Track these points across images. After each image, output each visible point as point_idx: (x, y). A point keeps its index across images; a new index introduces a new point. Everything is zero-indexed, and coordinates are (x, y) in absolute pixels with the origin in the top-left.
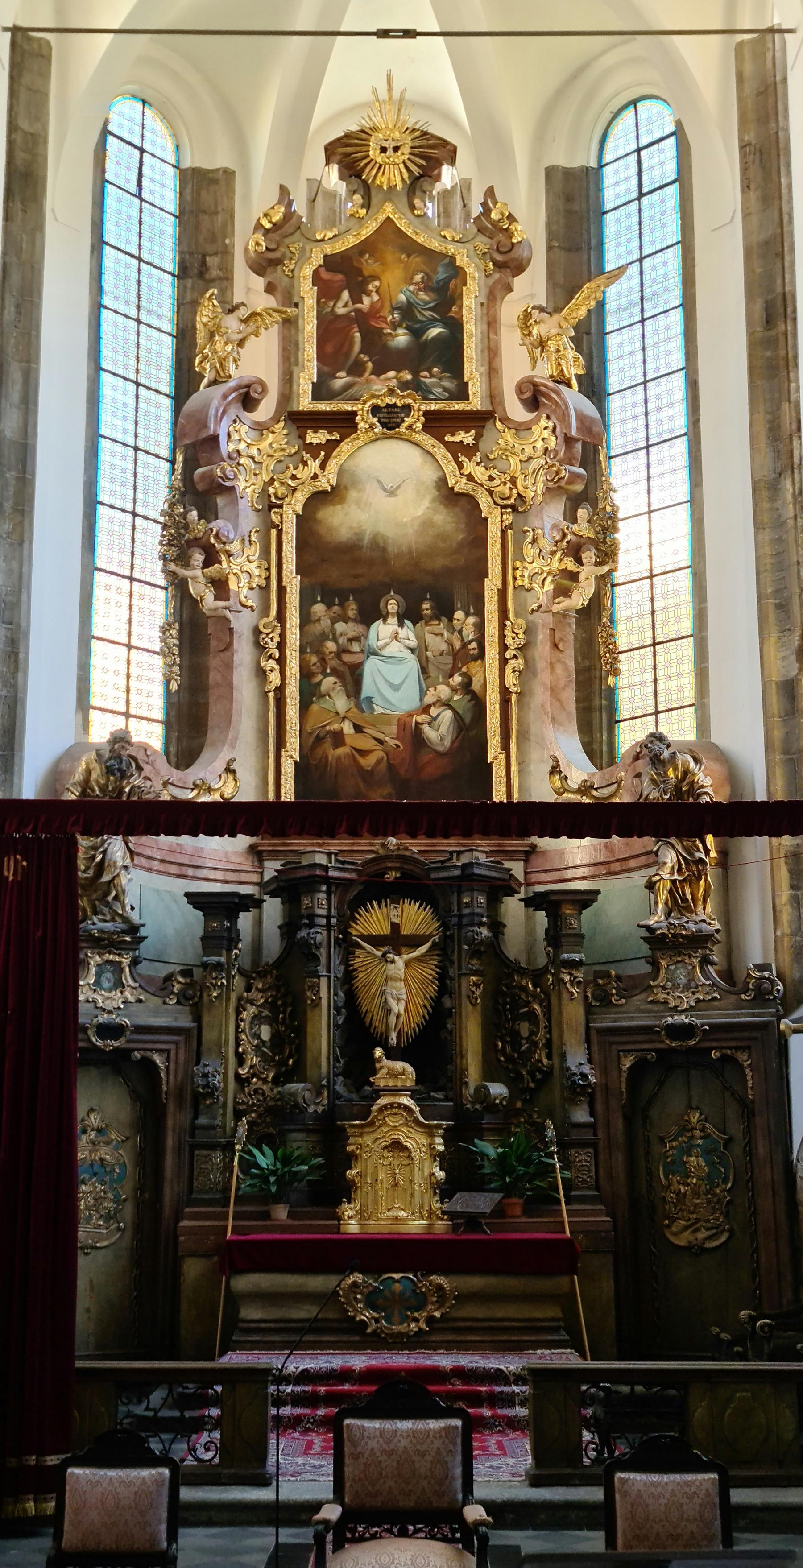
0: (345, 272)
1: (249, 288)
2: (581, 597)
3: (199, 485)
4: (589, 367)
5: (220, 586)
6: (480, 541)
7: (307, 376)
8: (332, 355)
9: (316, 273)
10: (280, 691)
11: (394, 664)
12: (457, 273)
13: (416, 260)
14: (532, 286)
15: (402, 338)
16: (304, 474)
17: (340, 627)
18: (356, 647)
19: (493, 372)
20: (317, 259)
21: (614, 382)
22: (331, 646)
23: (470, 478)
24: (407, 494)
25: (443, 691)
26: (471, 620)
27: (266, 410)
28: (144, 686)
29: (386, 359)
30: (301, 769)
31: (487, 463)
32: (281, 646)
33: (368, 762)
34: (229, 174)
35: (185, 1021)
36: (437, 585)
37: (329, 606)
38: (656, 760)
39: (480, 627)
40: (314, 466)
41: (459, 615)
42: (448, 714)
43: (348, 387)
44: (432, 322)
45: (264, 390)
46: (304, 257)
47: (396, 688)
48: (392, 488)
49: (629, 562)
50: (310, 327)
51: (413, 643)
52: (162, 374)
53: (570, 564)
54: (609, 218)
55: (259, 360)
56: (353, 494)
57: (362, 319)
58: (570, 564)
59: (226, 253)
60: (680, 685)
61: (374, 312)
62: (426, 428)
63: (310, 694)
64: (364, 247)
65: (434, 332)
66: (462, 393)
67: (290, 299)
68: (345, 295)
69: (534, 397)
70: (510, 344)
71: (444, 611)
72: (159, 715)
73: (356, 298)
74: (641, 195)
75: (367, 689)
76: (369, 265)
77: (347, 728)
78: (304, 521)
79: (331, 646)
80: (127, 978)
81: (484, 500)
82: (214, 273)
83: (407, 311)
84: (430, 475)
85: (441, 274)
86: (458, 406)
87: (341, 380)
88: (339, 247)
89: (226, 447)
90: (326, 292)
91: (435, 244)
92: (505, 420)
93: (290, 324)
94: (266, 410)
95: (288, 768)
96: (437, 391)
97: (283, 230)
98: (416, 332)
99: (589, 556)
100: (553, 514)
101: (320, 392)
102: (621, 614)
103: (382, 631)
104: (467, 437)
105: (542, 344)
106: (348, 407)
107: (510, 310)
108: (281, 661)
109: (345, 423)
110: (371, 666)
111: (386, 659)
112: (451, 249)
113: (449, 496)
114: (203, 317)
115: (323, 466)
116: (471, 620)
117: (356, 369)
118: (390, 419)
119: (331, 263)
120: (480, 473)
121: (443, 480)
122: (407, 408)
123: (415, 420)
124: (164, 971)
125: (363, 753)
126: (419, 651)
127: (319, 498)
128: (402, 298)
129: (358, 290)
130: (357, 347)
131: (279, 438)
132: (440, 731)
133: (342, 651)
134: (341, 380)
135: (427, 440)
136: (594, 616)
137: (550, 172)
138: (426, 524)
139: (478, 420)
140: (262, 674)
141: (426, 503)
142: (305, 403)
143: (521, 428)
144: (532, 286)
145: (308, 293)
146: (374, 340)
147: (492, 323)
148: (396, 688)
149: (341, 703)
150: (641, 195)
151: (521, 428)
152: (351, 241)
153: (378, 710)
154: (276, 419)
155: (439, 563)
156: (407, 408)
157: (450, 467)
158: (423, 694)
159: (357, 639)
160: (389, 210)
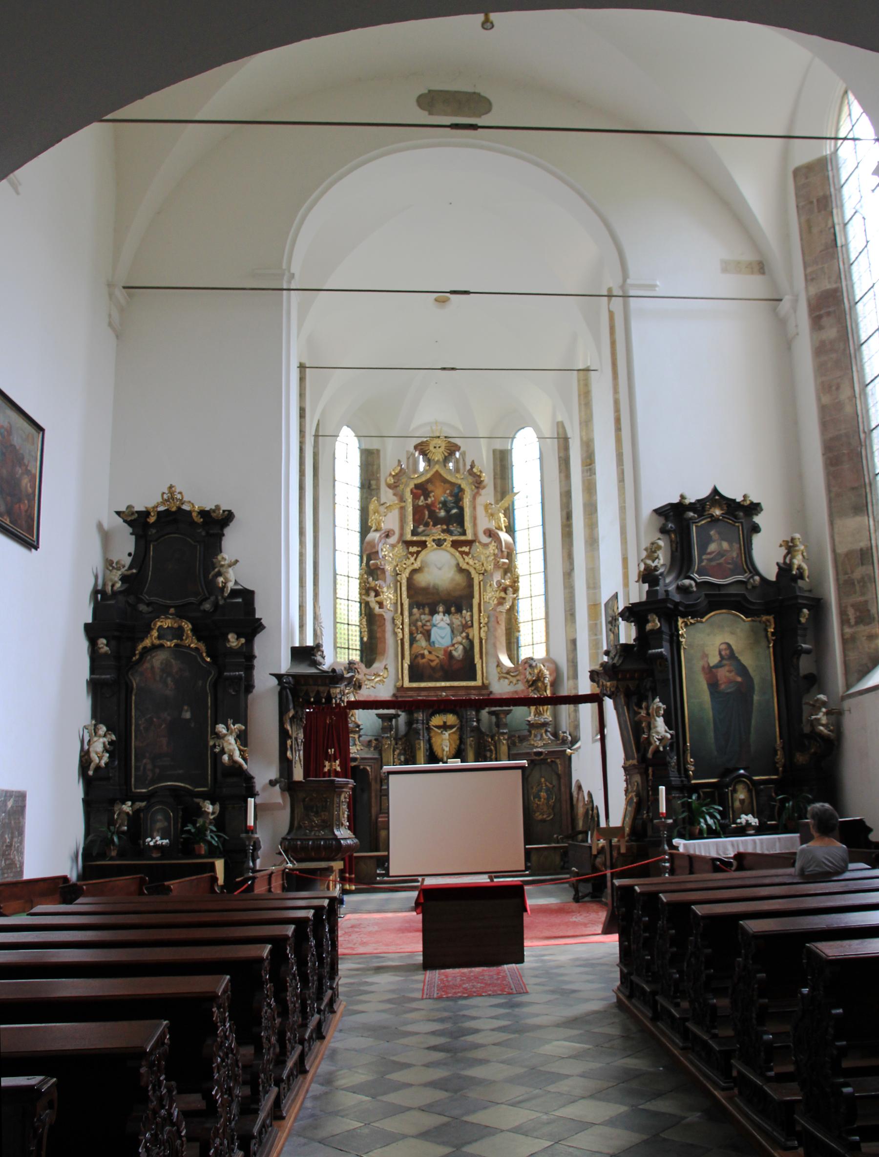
0: (422, 490)
1: (387, 495)
2: (507, 606)
3: (371, 569)
4: (509, 522)
5: (381, 604)
8: (418, 519)
9: (411, 491)
10: (402, 640)
11: (442, 629)
12: (461, 490)
13: (447, 485)
14: (487, 495)
15: (442, 513)
16: (408, 562)
17: (423, 617)
18: (428, 624)
19: (475, 525)
20: (412, 485)
21: (517, 527)
22: (419, 624)
23: (468, 563)
25: (459, 639)
26: (469, 613)
27: (393, 540)
28: (354, 638)
29: (437, 521)
30: (411, 667)
32: (402, 624)
33: (433, 664)
34: (378, 451)
35: (376, 756)
36: (458, 601)
37: (419, 609)
38: (531, 666)
39: (472, 616)
40: (412, 559)
41: (464, 612)
42: (461, 647)
43: (424, 531)
44: (453, 508)
45: (394, 534)
46: (407, 485)
47: (443, 638)
48: (439, 567)
50: (410, 509)
51: (448, 622)
52: (356, 525)
55: (391, 521)
56: (426, 569)
57: (428, 507)
58: (503, 594)
60: (541, 636)
61: (433, 504)
62: (452, 546)
63: (413, 640)
64: (429, 481)
65: (454, 511)
66: (464, 533)
67: (402, 499)
68: (422, 498)
69: (490, 533)
70: (479, 515)
71: (459, 610)
72: (358, 648)
73: (426, 499)
75: (433, 638)
76: (430, 487)
77: (426, 652)
78: (410, 580)
79: (419, 624)
80: (357, 742)
81: (473, 572)
82: (374, 487)
83: (444, 504)
84: (454, 562)
85: (456, 490)
86: (463, 538)
88: (419, 481)
89: (381, 555)
90: (415, 497)
91: (453, 480)
92: (480, 542)
93: (402, 509)
94: (393, 540)
95: (406, 666)
96: (456, 532)
97: (398, 476)
98: (448, 511)
100: (497, 576)
101: (414, 533)
102: (520, 609)
103: (438, 618)
104: (466, 549)
105: (492, 515)
106: (424, 538)
107: (481, 500)
108: (402, 629)
109: (423, 545)
110: (434, 631)
111: (440, 628)
112: (459, 482)
113: (460, 570)
114: (372, 507)
115: (415, 559)
116: (469, 613)
117: (426, 525)
118: (439, 543)
119: (417, 486)
121: (458, 564)
122: (445, 540)
123: (447, 544)
124: (368, 738)
125: (432, 661)
126: (451, 625)
127: (414, 571)
128: (442, 499)
130: (427, 516)
131: (400, 549)
132: (458, 653)
133: (424, 625)
134: (421, 528)
135: (452, 550)
136: (512, 612)
137: (494, 451)
138: (453, 580)
139: (469, 543)
140: (395, 634)
142: (409, 537)
143: (486, 546)
144: (487, 495)
145: (409, 498)
146: (433, 514)
147: (474, 508)
148: (443, 638)
149: (423, 643)
151: (486, 546)
152: (424, 479)
153: (437, 646)
154: (398, 542)
155: (457, 593)
156: (445, 540)
157: (461, 560)
159: (428, 621)
160: (437, 467)
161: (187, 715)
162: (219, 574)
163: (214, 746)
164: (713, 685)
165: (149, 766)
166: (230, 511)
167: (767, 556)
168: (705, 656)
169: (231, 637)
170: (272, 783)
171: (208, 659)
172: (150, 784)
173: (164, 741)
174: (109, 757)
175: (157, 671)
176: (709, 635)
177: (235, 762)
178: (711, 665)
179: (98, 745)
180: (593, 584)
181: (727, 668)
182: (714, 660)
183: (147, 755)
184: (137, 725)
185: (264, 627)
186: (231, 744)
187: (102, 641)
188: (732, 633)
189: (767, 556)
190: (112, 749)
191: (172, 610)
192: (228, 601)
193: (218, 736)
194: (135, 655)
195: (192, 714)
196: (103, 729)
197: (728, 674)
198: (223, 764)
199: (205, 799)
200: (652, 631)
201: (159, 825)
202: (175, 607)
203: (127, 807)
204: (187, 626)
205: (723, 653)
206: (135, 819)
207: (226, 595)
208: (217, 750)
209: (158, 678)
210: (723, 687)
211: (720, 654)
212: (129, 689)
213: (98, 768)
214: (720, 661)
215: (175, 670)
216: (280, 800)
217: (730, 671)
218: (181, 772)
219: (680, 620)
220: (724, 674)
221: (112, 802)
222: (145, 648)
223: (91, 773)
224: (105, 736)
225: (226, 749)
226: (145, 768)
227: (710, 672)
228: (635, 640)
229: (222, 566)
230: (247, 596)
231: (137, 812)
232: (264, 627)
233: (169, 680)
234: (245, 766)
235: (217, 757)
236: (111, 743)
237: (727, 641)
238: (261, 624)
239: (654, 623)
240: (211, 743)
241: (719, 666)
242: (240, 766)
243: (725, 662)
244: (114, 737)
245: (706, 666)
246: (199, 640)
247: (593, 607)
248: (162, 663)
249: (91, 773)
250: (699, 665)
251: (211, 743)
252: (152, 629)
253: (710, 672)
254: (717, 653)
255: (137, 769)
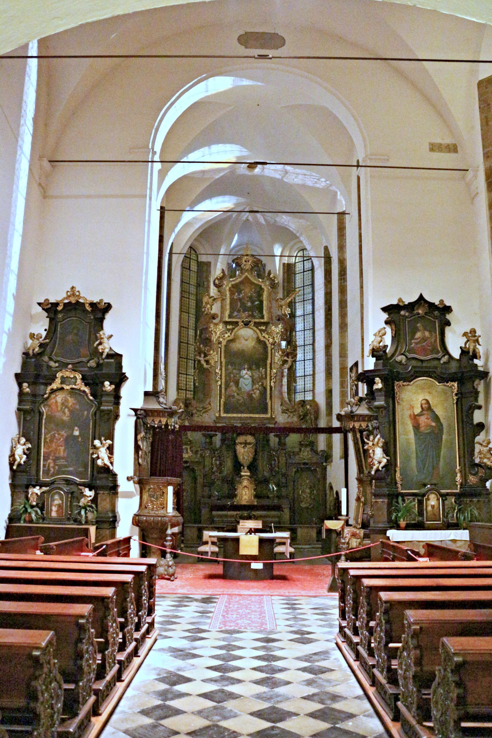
1: (213, 291)
4: (292, 311)
5: (207, 362)
6: (267, 352)
7: (227, 313)
12: (262, 289)
13: (253, 286)
15: (249, 304)
16: (226, 335)
17: (234, 371)
20: (230, 285)
23: (264, 337)
24: (250, 340)
25: (257, 386)
30: (225, 404)
31: (268, 334)
37: (232, 366)
39: (266, 372)
44: (256, 301)
45: (217, 317)
46: (228, 285)
47: (246, 385)
49: (300, 356)
50: (228, 301)
51: (250, 374)
53: (286, 358)
54: (297, 275)
57: (240, 300)
59: (208, 281)
61: (243, 298)
63: (227, 386)
64: (241, 283)
65: (257, 303)
66: (263, 317)
71: (258, 367)
74: (304, 272)
75: (240, 385)
76: (242, 287)
77: (236, 394)
80: (189, 451)
83: (251, 298)
84: (255, 336)
85: (258, 290)
86: (262, 321)
87: (235, 314)
90: (232, 293)
95: (222, 403)
98: (253, 302)
99: (290, 357)
101: (230, 316)
103: (244, 372)
104: (264, 328)
106: (237, 320)
108: (221, 378)
110: (241, 380)
111: (244, 379)
112: (260, 284)
113: (259, 341)
117: (239, 311)
120: (267, 336)
121: (258, 338)
122: (250, 322)
123: (252, 324)
126: (252, 377)
129: (240, 293)
131: (221, 326)
132: (256, 395)
135: (255, 328)
137: (284, 264)
138: (254, 347)
139: (266, 324)
141: (254, 343)
142: (227, 319)
146: (243, 305)
148: (246, 385)
149: (234, 388)
150: (304, 272)
154: (220, 321)
156: (250, 322)
158: (253, 387)
160: (246, 274)
161: (77, 433)
162: (100, 344)
163: (93, 454)
164: (416, 427)
165: (52, 465)
166: (109, 303)
167: (455, 345)
168: (412, 407)
169: (107, 383)
170: (129, 479)
171: (91, 398)
172: (52, 476)
173: (62, 448)
174: (27, 458)
175: (59, 404)
176: (415, 393)
177: (105, 464)
178: (416, 414)
179: (19, 451)
180: (343, 355)
181: (425, 416)
182: (418, 410)
183: (51, 458)
184: (45, 438)
185: (128, 378)
186: (103, 453)
187: (25, 385)
188: (429, 393)
189: (455, 345)
190: (28, 453)
191: (70, 366)
192: (106, 360)
193: (95, 447)
194: (46, 394)
195: (80, 433)
196: (23, 440)
197: (426, 420)
198: (98, 466)
199: (86, 487)
200: (377, 389)
201: (56, 502)
202: (72, 364)
203: (37, 490)
204: (79, 376)
205: (424, 406)
206: (41, 497)
207: (104, 356)
208: (95, 456)
209: (59, 409)
210: (422, 429)
211: (422, 407)
212: (41, 414)
213: (19, 465)
214: (422, 412)
215: (70, 404)
216: (133, 490)
217: (427, 419)
218: (71, 469)
219: (396, 383)
220: (423, 420)
221: (27, 487)
222: (52, 389)
223: (15, 467)
224: (24, 444)
225: (100, 456)
226: (49, 466)
227: (415, 418)
228: (366, 395)
229: (102, 338)
230: (117, 358)
231: (43, 493)
232: (128, 378)
233: (66, 410)
234: (111, 468)
235: (94, 461)
236: (28, 449)
237: (427, 398)
238: (125, 376)
239: (379, 385)
240: (91, 452)
241: (420, 415)
242: (108, 468)
243: (424, 412)
244: (30, 446)
245: (412, 414)
246: (86, 385)
247: (343, 369)
248: (62, 400)
249: (15, 467)
250: (407, 413)
251: (91, 452)
252: (57, 378)
253: (415, 418)
254: (419, 406)
255: (44, 466)
